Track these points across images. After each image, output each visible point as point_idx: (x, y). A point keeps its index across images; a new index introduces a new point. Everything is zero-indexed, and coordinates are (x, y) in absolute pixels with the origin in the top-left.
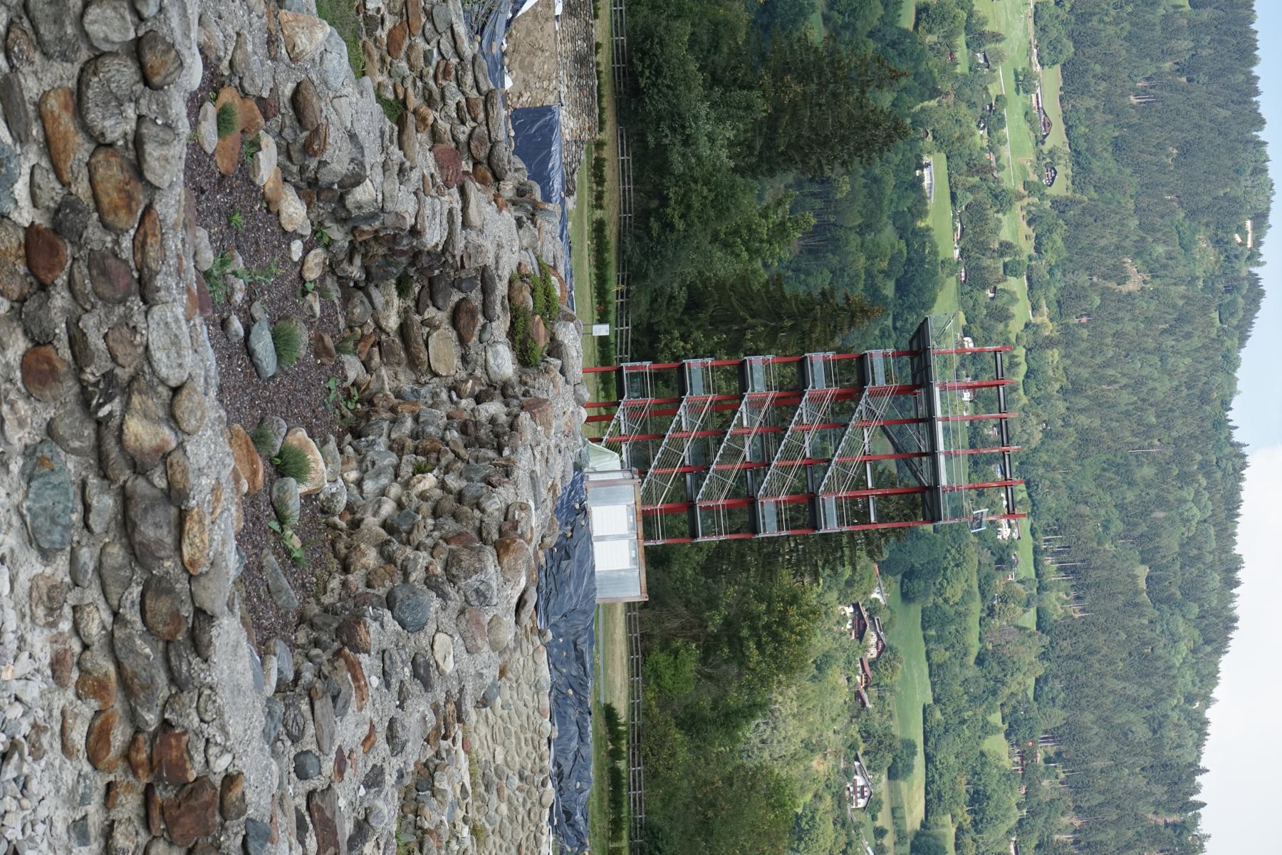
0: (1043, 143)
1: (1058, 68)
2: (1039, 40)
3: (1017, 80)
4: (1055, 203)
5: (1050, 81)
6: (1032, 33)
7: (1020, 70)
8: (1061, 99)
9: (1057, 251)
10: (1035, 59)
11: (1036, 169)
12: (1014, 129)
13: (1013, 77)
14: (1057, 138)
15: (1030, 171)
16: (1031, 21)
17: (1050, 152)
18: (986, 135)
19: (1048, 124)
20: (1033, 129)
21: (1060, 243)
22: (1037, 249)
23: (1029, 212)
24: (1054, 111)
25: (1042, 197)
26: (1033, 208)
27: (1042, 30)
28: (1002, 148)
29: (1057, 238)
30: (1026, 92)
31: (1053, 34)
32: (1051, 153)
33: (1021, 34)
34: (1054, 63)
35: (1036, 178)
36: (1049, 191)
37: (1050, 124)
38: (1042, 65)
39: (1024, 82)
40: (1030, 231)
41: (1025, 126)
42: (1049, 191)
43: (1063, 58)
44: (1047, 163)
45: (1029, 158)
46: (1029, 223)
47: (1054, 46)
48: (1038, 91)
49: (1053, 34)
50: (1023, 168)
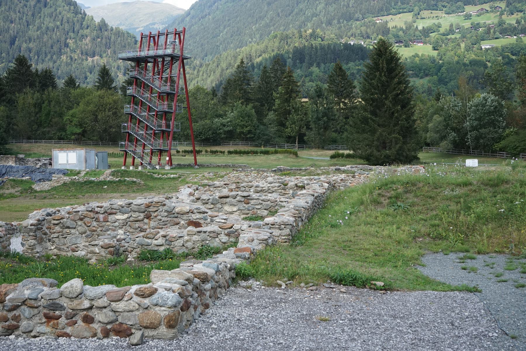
0: (488, 11)
1: (465, 7)
2: (456, 12)
3: (467, 19)
4: (507, 6)
5: (470, 9)
6: (455, 15)
7: (464, 18)
8: (475, 5)
9: (522, 6)
10: (462, 14)
11: (496, 13)
12: (481, 20)
13: (466, 20)
14: (487, 7)
15: (496, 14)
16: (450, 15)
17: (491, 8)
18: (481, 28)
19: (482, 9)
20: (483, 14)
21: (520, 5)
22: (521, 12)
23: (509, 15)
24: (479, 7)
25: (505, 11)
26: (508, 13)
27: (453, 12)
28: (487, 23)
29: (518, 5)
30: (471, 16)
31: (454, 8)
32: (491, 8)
33: (453, 18)
34: (464, 8)
35: (499, 13)
36: (503, 8)
37: (482, 9)
38: (464, 11)
39: (468, 17)
40: (515, 14)
41: (482, 16)
42: (503, 8)
43: (462, 5)
44: (494, 9)
45: (492, 15)
46: (513, 14)
47: (458, 8)
48: (471, 13)
49: (454, 8)
50: (495, 17)
